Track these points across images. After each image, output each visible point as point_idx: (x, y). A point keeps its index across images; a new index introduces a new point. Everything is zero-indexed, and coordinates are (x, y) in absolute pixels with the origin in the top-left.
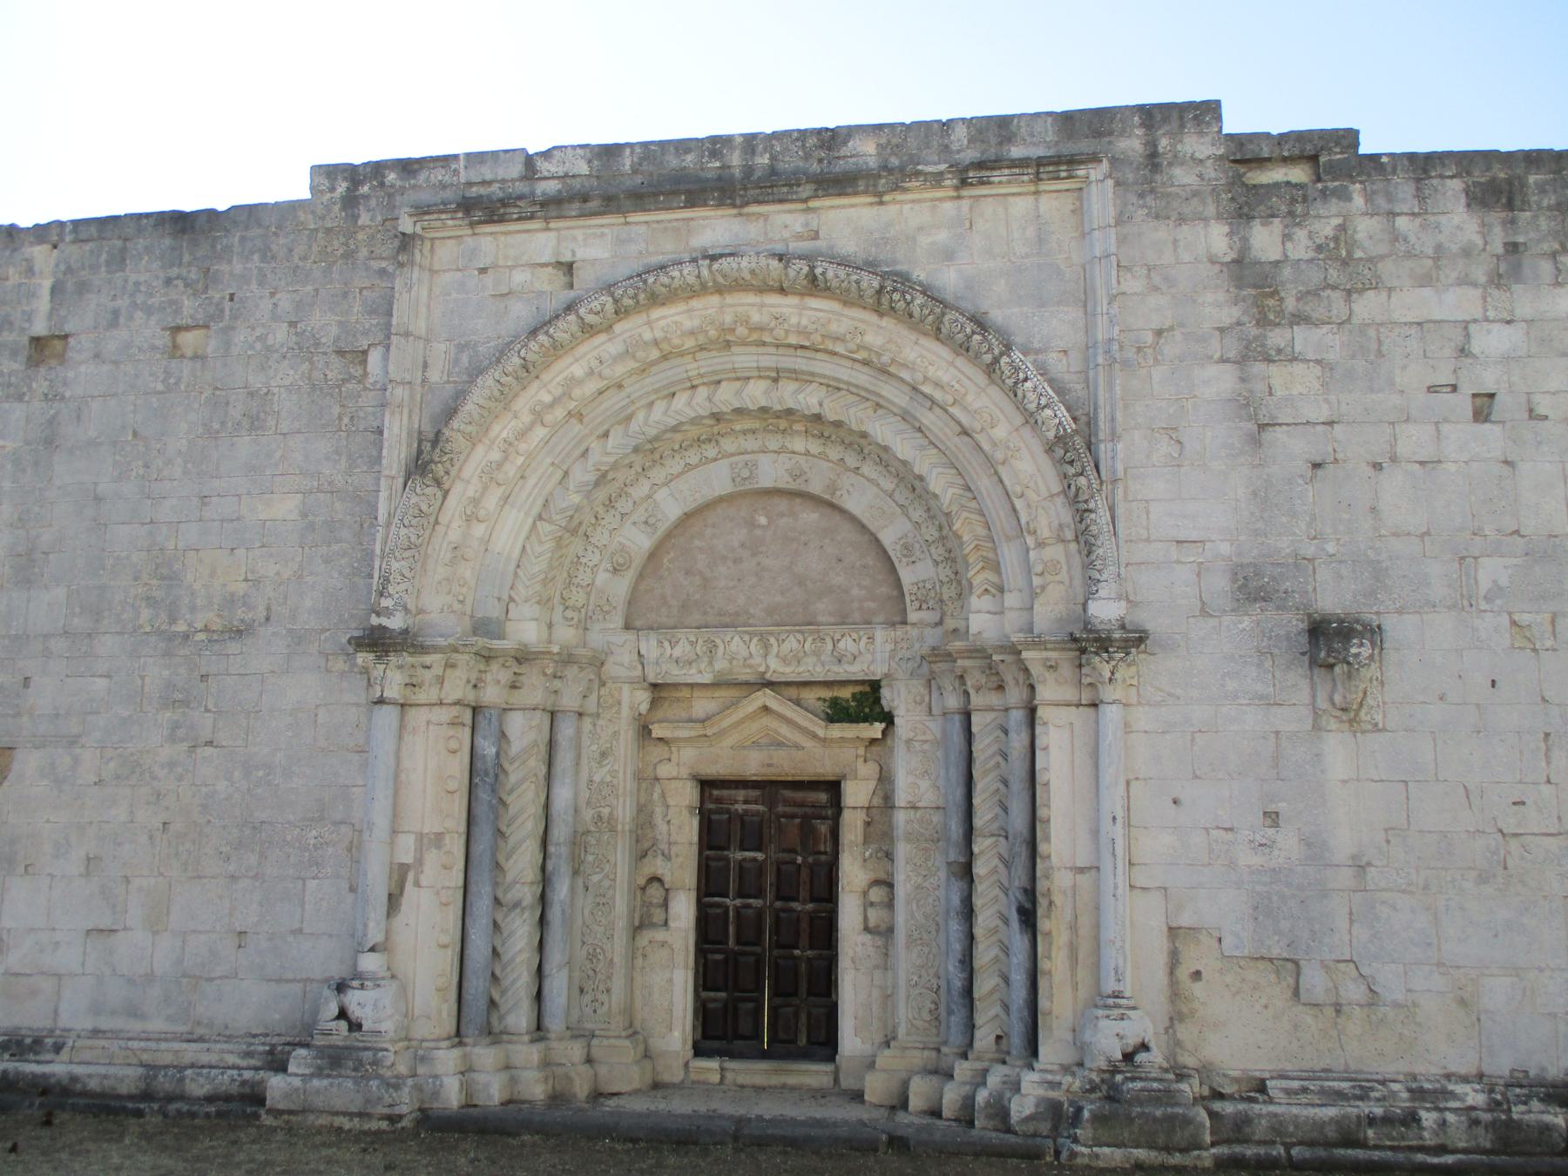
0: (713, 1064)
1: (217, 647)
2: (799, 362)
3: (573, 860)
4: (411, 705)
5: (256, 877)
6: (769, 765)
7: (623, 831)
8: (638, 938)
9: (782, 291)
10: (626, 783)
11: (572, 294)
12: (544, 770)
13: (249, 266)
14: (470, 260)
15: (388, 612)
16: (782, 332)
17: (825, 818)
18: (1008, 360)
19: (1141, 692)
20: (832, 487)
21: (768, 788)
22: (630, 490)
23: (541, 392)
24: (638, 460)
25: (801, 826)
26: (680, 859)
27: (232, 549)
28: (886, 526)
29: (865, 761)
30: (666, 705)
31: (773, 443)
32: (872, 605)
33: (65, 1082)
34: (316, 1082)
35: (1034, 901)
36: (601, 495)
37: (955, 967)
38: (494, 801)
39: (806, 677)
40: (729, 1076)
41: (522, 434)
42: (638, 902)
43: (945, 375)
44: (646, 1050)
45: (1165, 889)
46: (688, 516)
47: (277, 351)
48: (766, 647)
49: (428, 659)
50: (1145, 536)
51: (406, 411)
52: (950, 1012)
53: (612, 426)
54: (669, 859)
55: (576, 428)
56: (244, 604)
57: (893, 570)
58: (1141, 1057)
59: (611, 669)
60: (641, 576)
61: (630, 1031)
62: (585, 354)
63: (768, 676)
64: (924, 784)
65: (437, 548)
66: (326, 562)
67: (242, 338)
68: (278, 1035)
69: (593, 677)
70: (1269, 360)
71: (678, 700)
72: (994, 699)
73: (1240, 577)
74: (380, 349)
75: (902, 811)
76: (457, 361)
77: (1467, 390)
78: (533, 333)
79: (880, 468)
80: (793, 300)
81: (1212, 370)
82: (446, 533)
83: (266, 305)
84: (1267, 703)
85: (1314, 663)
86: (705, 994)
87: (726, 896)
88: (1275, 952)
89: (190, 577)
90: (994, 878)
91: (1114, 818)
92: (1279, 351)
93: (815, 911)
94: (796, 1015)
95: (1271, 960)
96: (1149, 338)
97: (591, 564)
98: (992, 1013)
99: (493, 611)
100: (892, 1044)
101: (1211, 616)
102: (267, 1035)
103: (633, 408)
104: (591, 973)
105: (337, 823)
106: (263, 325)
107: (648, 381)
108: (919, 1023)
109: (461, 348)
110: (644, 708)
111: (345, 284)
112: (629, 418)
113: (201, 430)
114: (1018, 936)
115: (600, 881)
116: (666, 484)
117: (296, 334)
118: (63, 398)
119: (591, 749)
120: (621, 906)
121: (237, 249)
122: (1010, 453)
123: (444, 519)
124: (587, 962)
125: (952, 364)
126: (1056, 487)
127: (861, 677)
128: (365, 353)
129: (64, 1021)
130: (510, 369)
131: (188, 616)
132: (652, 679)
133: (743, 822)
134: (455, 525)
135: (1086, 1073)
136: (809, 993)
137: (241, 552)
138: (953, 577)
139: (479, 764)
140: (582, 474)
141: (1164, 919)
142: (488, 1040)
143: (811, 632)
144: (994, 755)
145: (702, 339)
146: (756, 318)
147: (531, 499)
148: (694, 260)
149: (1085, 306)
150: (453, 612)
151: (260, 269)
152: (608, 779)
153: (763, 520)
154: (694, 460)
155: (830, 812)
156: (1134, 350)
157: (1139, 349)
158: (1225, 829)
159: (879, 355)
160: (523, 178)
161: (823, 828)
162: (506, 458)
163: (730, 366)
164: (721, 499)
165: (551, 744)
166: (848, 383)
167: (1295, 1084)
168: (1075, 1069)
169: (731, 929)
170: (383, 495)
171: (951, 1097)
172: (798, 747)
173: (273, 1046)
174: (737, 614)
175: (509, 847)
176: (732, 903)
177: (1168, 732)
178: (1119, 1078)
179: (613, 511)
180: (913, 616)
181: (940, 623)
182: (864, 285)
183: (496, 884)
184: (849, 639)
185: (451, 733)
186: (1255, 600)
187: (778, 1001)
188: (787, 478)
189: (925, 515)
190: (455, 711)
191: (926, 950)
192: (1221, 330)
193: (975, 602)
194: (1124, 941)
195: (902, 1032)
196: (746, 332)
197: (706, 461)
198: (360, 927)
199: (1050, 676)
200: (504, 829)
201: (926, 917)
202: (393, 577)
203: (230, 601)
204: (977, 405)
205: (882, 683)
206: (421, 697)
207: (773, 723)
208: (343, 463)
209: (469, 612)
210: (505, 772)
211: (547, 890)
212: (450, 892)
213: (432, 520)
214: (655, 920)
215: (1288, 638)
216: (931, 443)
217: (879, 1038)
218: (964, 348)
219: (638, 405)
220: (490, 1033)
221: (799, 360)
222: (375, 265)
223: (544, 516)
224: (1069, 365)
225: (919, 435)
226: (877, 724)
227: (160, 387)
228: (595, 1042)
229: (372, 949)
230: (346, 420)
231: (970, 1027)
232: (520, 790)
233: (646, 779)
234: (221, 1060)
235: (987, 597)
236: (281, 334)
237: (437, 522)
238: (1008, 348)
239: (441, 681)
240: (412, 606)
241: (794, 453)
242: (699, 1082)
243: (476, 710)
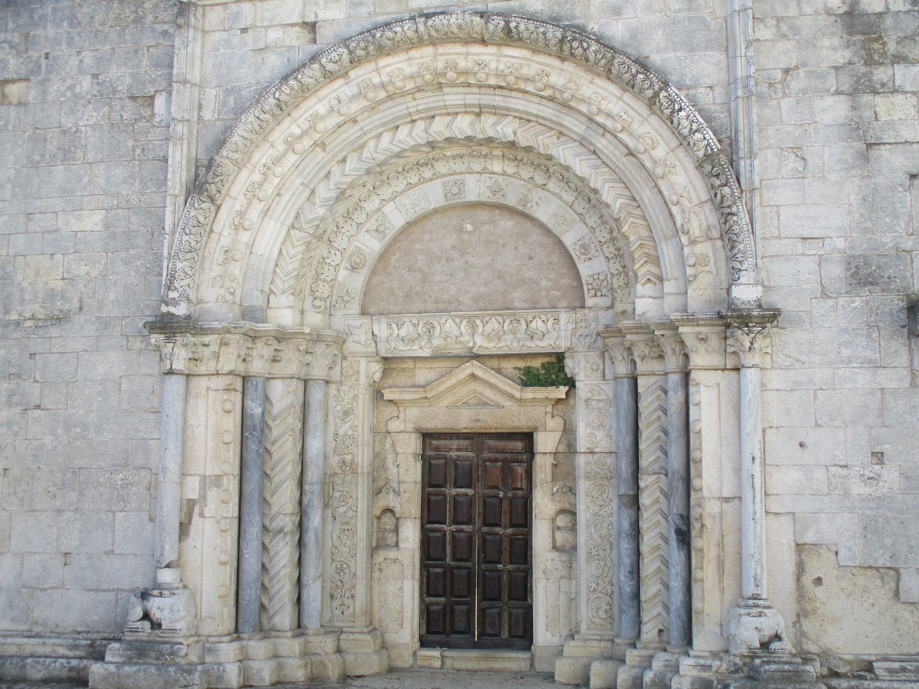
0: (436, 653)
1: (41, 332)
2: (498, 100)
3: (324, 497)
4: (194, 375)
5: (76, 510)
6: (477, 421)
7: (363, 473)
8: (375, 556)
9: (483, 42)
10: (363, 435)
11: (315, 48)
12: (300, 425)
13: (59, 31)
14: (234, 22)
15: (175, 302)
16: (484, 76)
17: (521, 462)
18: (666, 94)
19: (774, 359)
20: (525, 201)
21: (475, 438)
22: (364, 205)
23: (291, 127)
24: (370, 181)
25: (503, 469)
26: (408, 495)
27: (52, 255)
28: (568, 231)
29: (553, 417)
30: (395, 374)
31: (477, 166)
32: (557, 293)
34: (127, 669)
35: (688, 525)
36: (341, 208)
37: (625, 576)
38: (261, 450)
39: (505, 351)
40: (448, 662)
41: (278, 160)
42: (375, 529)
43: (615, 108)
44: (383, 642)
45: (793, 514)
46: (410, 224)
47: (83, 98)
48: (474, 327)
49: (206, 339)
50: (777, 234)
51: (185, 142)
52: (622, 612)
53: (349, 153)
54: (399, 495)
55: (320, 154)
56: (63, 297)
57: (573, 266)
58: (775, 646)
59: (350, 346)
60: (374, 272)
61: (371, 628)
62: (327, 95)
63: (475, 350)
64: (600, 434)
65: (212, 251)
67: (55, 88)
68: (97, 632)
69: (336, 352)
70: (875, 92)
71: (404, 370)
72: (656, 366)
73: (853, 266)
74: (164, 94)
75: (583, 455)
76: (225, 103)
78: (285, 78)
79: (562, 184)
80: (492, 49)
81: (830, 100)
82: (219, 239)
83: (74, 61)
84: (875, 366)
86: (428, 599)
87: (445, 523)
88: (881, 562)
89: (19, 277)
90: (656, 507)
91: (753, 458)
92: (883, 85)
93: (513, 535)
94: (500, 615)
95: (877, 569)
96: (779, 75)
97: (333, 264)
98: (655, 612)
99: (257, 300)
100: (576, 637)
101: (830, 297)
102: (89, 632)
103: (365, 138)
104: (339, 584)
105: (136, 468)
106: (72, 78)
107: (376, 117)
108: (596, 620)
109: (228, 92)
110: (377, 376)
111: (136, 44)
112: (362, 147)
113: (25, 162)
114: (676, 552)
115: (345, 512)
116: (393, 199)
117: (98, 84)
119: (336, 409)
120: (362, 530)
121: (50, 17)
122: (668, 169)
123: (217, 228)
124: (336, 575)
125: (620, 98)
126: (704, 196)
127: (549, 350)
128: (152, 98)
130: (267, 108)
131: (19, 308)
132: (383, 353)
133: (456, 465)
134: (226, 233)
135: (732, 658)
136: (510, 599)
137: (59, 257)
138: (621, 269)
139: (248, 422)
140: (325, 192)
141: (792, 538)
142: (258, 636)
143: (509, 315)
144: (656, 410)
145: (419, 82)
146: (462, 64)
147: (285, 212)
148: (412, 18)
149: (727, 51)
150: (226, 301)
151: (68, 33)
152: (350, 432)
153: (469, 227)
154: (414, 180)
155: (525, 457)
156: (767, 85)
157: (771, 85)
158: (841, 466)
159: (562, 92)
161: (520, 469)
162: (265, 180)
163: (442, 104)
164: (436, 211)
165: (305, 406)
166: (537, 116)
167: (896, 665)
168: (722, 655)
169: (448, 549)
170: (169, 210)
172: (502, 407)
173: (94, 640)
174: (450, 302)
175: (273, 486)
176: (448, 528)
177: (795, 390)
178: (757, 661)
179: (351, 222)
180: (590, 302)
181: (612, 307)
182: (550, 35)
183: (263, 515)
184: (540, 322)
185: (226, 397)
186: (865, 284)
187: (485, 604)
188: (488, 193)
189: (599, 221)
190: (228, 379)
191: (602, 563)
192: (837, 68)
193: (640, 289)
194: (761, 555)
195: (583, 627)
196: (455, 75)
197: (423, 181)
198: (158, 549)
199: (701, 347)
200: (269, 472)
201: (602, 537)
202: (179, 274)
203: (51, 295)
204: (641, 131)
205: (567, 355)
206: (202, 369)
207: (480, 388)
209: (238, 301)
210: (270, 429)
211: (304, 519)
212: (228, 521)
213: (208, 229)
214: (388, 543)
215: (891, 313)
216: (604, 163)
217: (565, 632)
218: (630, 86)
219: (369, 136)
220: (261, 630)
221: (497, 98)
222: (159, 28)
223: (296, 225)
224: (714, 98)
225: (594, 157)
226: (562, 387)
228: (343, 636)
229: (168, 566)
230: (138, 151)
231: (638, 622)
232: (281, 441)
233: (379, 433)
234: (54, 651)
235: (649, 285)
236: (86, 84)
237: (211, 231)
238: (666, 85)
239: (217, 356)
240: (192, 297)
241: (494, 173)
242: (424, 667)
243: (245, 379)
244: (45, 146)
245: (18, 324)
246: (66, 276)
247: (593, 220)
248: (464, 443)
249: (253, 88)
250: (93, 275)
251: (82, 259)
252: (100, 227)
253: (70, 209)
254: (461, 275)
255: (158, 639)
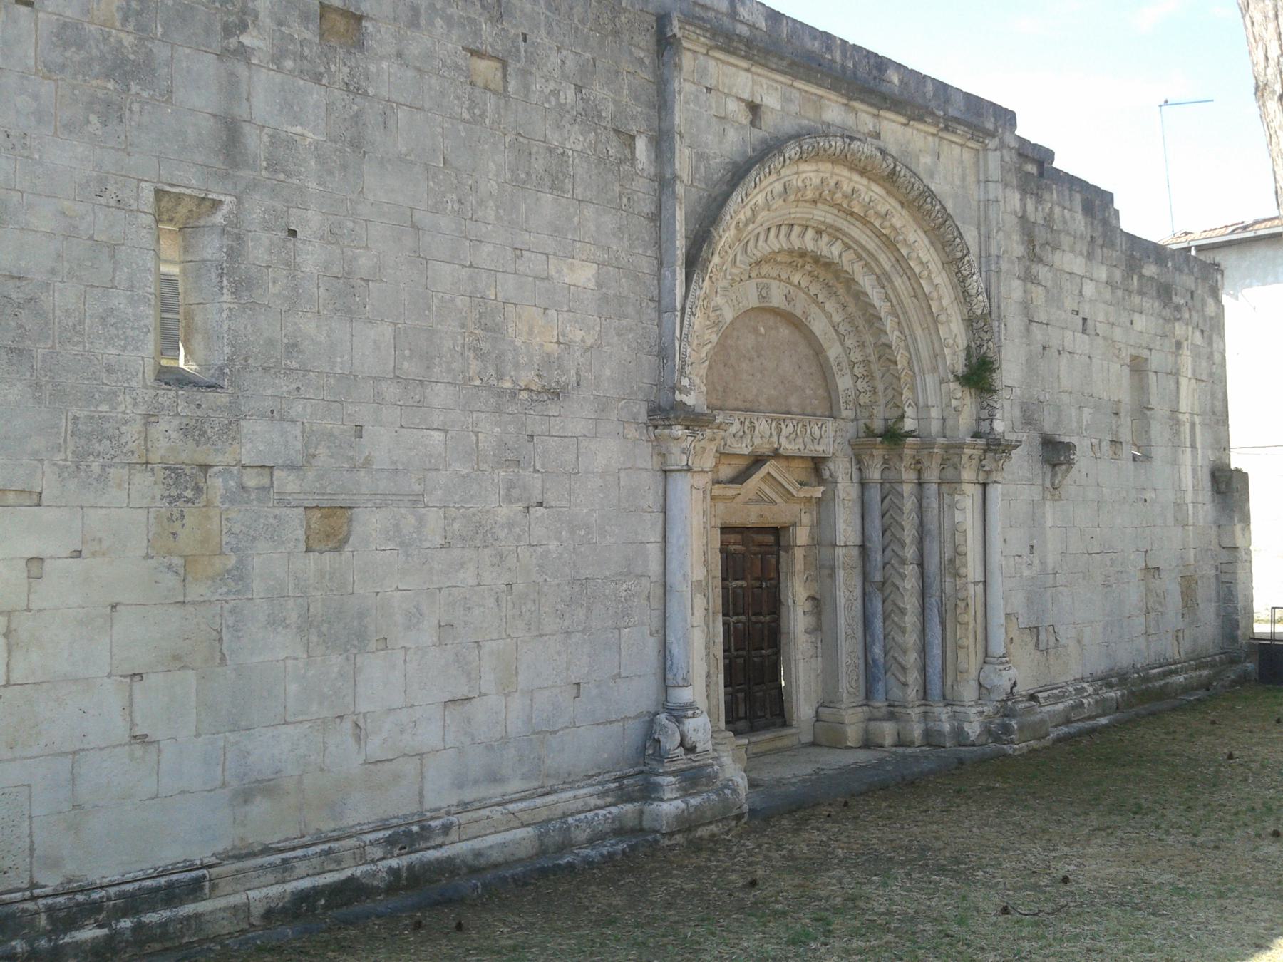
1: (539, 408)
27: (545, 309)
33: (470, 859)
64: (849, 529)
66: (619, 335)
77: (1081, 315)
79: (837, 306)
83: (555, 59)
85: (1046, 461)
102: (599, 774)
105: (638, 576)
113: (508, 176)
117: (582, 99)
118: (365, 94)
128: (633, 138)
129: (431, 801)
131: (513, 373)
137: (552, 313)
148: (842, 137)
153: (762, 330)
160: (728, 15)
164: (753, 309)
171: (917, 731)
172: (774, 503)
180: (845, 413)
189: (856, 344)
203: (548, 361)
208: (626, 243)
221: (845, 223)
227: (466, 116)
230: (625, 200)
234: (586, 804)
244: (530, 162)
245: (514, 395)
246: (561, 340)
247: (850, 341)
248: (738, 537)
249: (717, 160)
250: (589, 344)
251: (577, 321)
252: (592, 285)
253: (561, 254)
254: (759, 376)
255: (694, 764)
